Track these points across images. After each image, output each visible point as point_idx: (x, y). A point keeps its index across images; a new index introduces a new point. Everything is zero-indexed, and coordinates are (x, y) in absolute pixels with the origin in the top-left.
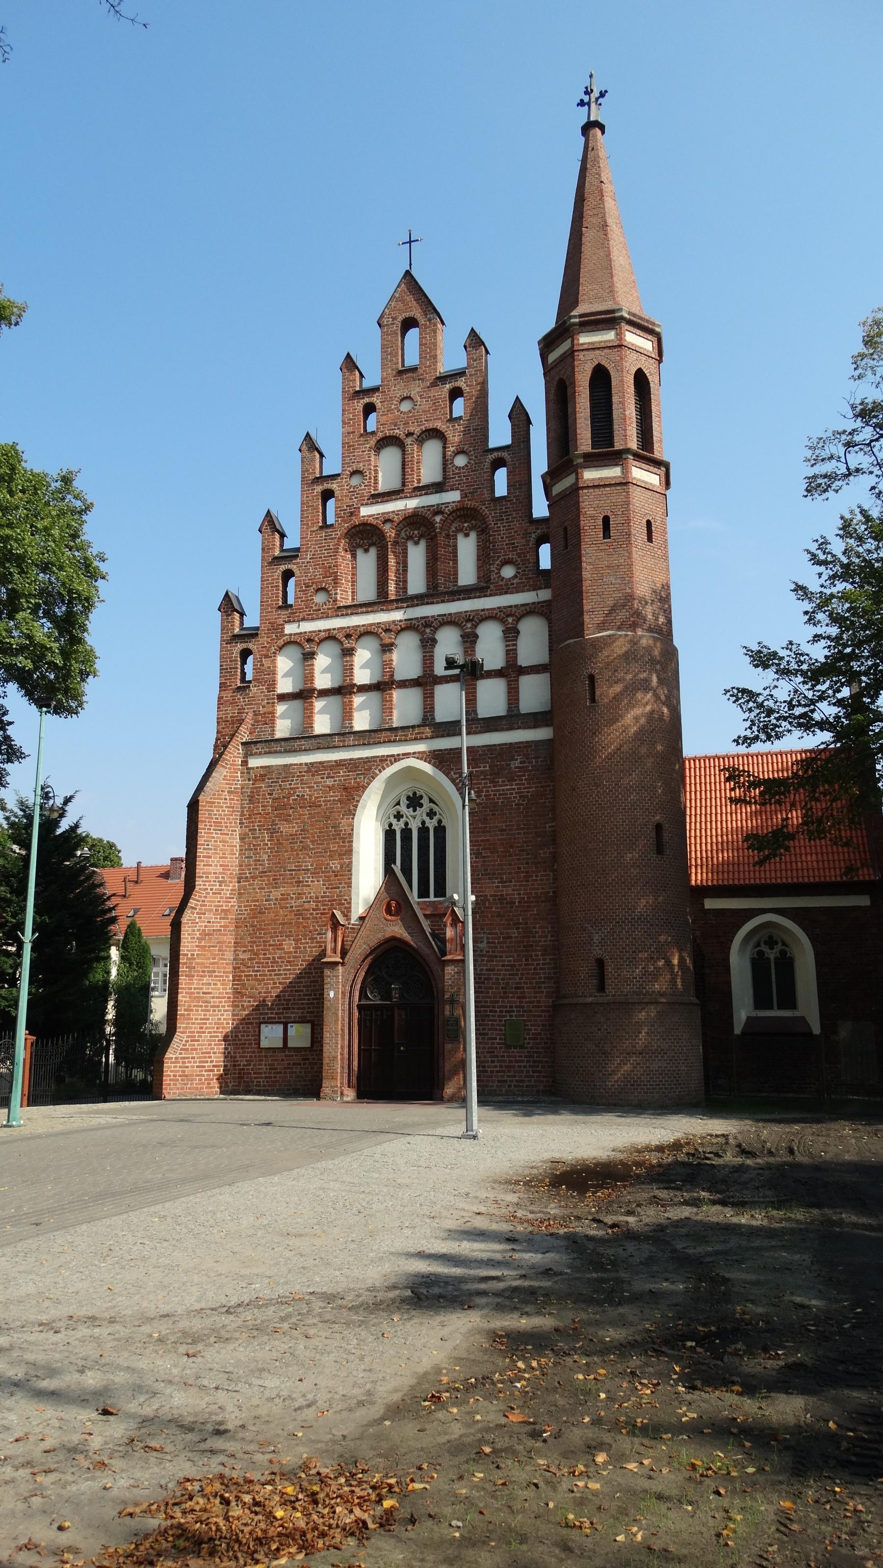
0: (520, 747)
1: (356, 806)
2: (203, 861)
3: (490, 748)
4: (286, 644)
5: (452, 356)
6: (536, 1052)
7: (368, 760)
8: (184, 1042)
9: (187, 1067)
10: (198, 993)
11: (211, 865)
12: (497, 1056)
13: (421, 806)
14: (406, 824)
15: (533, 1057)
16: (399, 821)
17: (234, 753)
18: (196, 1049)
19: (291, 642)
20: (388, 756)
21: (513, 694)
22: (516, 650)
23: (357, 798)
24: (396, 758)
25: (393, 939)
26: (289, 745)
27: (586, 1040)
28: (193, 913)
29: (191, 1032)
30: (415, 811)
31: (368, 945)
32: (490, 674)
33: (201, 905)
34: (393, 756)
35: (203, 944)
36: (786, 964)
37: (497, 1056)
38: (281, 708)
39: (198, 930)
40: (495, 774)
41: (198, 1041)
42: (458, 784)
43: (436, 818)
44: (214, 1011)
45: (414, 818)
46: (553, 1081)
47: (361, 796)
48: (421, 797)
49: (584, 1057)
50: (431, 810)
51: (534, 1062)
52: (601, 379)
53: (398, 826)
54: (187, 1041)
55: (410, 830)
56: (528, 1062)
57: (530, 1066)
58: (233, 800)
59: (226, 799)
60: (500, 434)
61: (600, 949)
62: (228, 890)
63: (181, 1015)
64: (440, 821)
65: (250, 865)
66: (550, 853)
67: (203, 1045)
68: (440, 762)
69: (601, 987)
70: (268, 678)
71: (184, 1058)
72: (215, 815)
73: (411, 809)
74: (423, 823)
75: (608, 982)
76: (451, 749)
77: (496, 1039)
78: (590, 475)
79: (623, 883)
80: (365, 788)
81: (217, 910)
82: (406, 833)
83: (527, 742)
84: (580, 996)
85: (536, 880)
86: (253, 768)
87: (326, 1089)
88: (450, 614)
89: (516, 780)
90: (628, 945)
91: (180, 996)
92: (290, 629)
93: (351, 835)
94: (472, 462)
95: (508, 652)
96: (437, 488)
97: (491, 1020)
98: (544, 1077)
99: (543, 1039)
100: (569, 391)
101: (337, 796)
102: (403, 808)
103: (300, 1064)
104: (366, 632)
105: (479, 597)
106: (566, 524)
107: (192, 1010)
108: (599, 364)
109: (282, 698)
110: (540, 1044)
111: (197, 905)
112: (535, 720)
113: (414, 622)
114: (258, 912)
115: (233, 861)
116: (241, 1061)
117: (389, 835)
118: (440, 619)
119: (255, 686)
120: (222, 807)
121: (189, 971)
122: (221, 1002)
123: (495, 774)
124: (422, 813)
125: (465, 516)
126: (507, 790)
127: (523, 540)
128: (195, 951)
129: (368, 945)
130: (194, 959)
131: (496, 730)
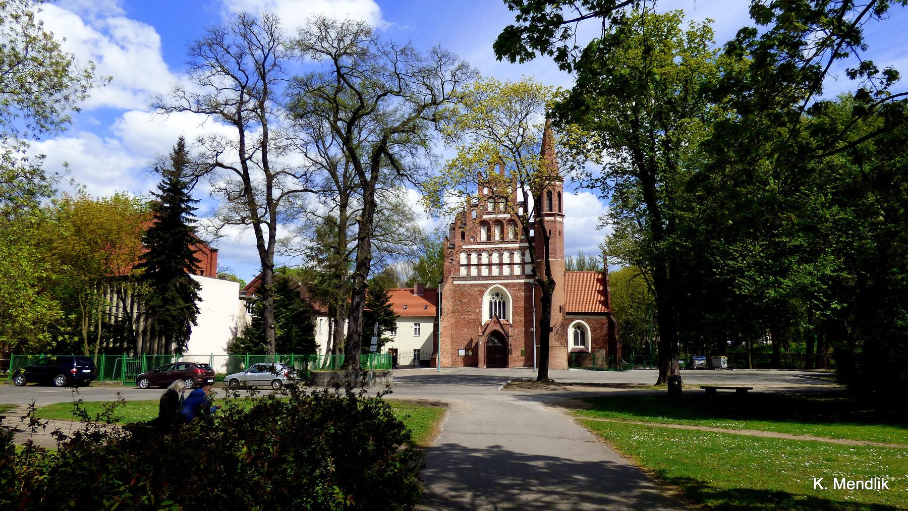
17: (450, 280)
26: (464, 278)
36: (583, 334)
38: (462, 268)
40: (519, 290)
52: (550, 194)
78: (546, 218)
82: (495, 303)
87: (480, 365)
92: (464, 247)
96: (505, 213)
104: (485, 250)
112: (528, 277)
114: (457, 321)
115: (450, 308)
117: (491, 303)
123: (519, 290)
125: (511, 221)
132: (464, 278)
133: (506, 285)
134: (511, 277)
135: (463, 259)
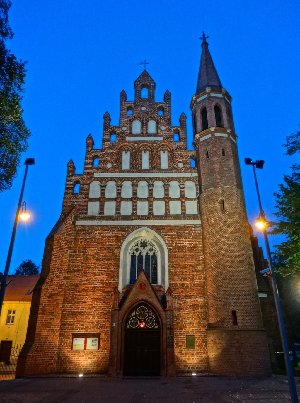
0: (188, 226)
1: (122, 244)
2: (53, 262)
3: (177, 226)
4: (95, 180)
5: (159, 97)
6: (200, 352)
7: (128, 227)
8: (37, 347)
9: (37, 360)
10: (46, 323)
11: (56, 265)
12: (183, 354)
13: (147, 246)
14: (140, 253)
15: (199, 354)
16: (137, 252)
18: (42, 351)
19: (97, 179)
20: (135, 226)
21: (183, 207)
22: (184, 192)
23: (122, 241)
24: (139, 227)
25: (142, 300)
26: (93, 218)
27: (231, 347)
28: (47, 285)
29: (40, 342)
30: (144, 248)
31: (131, 302)
32: (174, 199)
33: (51, 282)
34: (138, 226)
35: (50, 300)
37: (183, 354)
39: (49, 293)
40: (179, 236)
41: (43, 347)
42: (164, 238)
43: (153, 252)
44: (52, 332)
45: (144, 251)
46: (208, 366)
47: (124, 240)
48: (147, 243)
49: (231, 355)
50: (151, 248)
51: (199, 356)
53: (137, 254)
54: (38, 347)
55: (142, 256)
56: (197, 356)
57: (198, 359)
58: (68, 238)
59: (65, 237)
60: (175, 122)
61: (234, 307)
62: (62, 276)
63: (37, 333)
64: (154, 253)
65: (73, 266)
66: (202, 267)
67: (45, 349)
68: (157, 230)
69: (235, 322)
70: (85, 192)
71: (37, 355)
72: (60, 243)
73: (142, 248)
74: (147, 253)
75: (238, 321)
76: (161, 225)
77: (182, 346)
78: (217, 135)
79: (241, 279)
80: (126, 237)
81: (57, 284)
82: (140, 257)
83: (191, 225)
84: (226, 327)
85: (197, 278)
86: (77, 226)
88: (159, 177)
89: (187, 238)
90: (245, 305)
91: (37, 324)
92: (96, 175)
93: (119, 255)
94: (167, 129)
95: (181, 193)
96: (155, 135)
97: (180, 337)
98: (204, 364)
99: (202, 346)
100: (207, 109)
101: (114, 239)
102: (139, 247)
103: (92, 358)
104: (128, 179)
105: (170, 173)
106: (207, 150)
107: (42, 331)
108: (217, 103)
109: (92, 200)
110: (202, 348)
111: (49, 281)
112: (194, 217)
113: (145, 178)
116: (62, 357)
117: (133, 257)
118: (155, 178)
119: (80, 195)
120: (63, 240)
121: (43, 312)
122: (55, 328)
124: (147, 249)
126: (184, 242)
127: (186, 156)
128: (46, 302)
129: (131, 302)
130: (46, 306)
131: (179, 219)
132: (93, 218)
133: (158, 229)
134: (167, 216)
135: (95, 190)
